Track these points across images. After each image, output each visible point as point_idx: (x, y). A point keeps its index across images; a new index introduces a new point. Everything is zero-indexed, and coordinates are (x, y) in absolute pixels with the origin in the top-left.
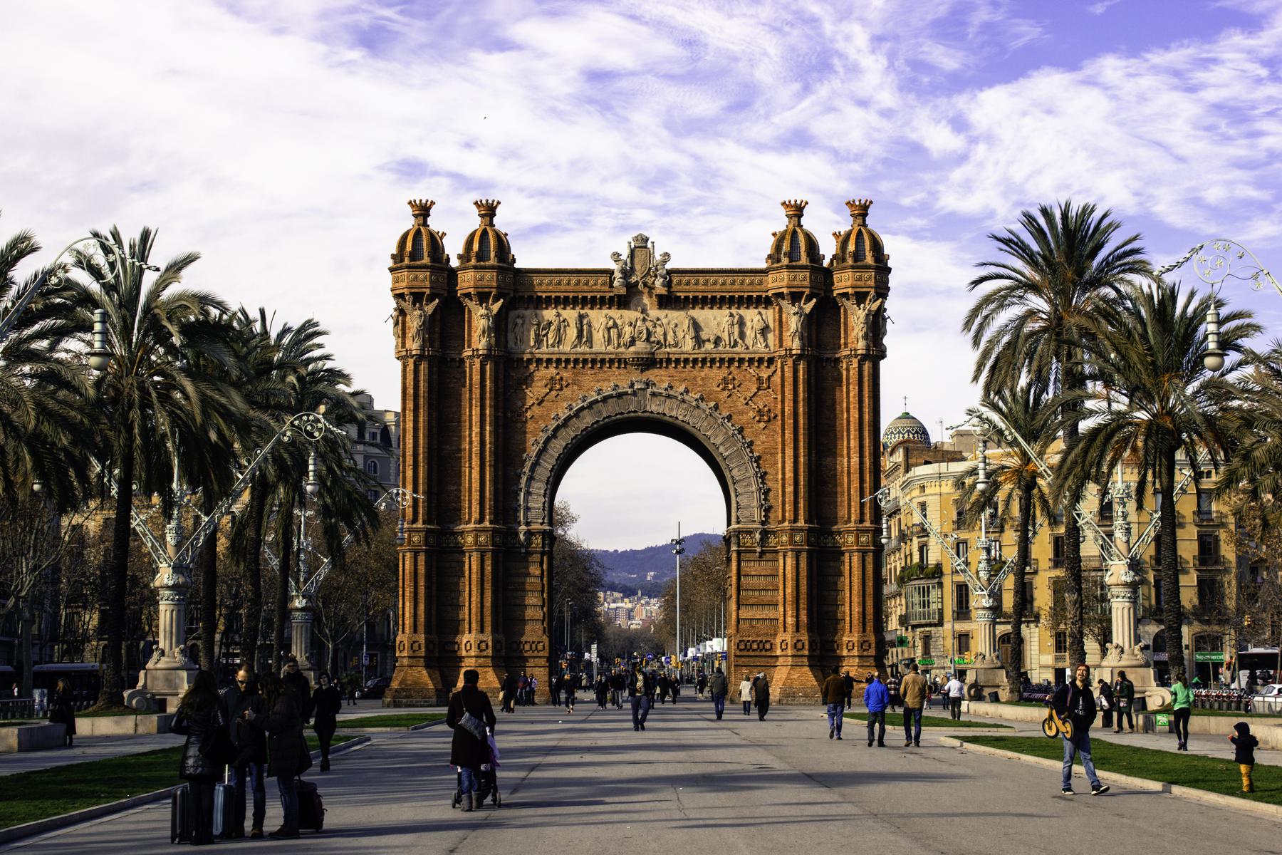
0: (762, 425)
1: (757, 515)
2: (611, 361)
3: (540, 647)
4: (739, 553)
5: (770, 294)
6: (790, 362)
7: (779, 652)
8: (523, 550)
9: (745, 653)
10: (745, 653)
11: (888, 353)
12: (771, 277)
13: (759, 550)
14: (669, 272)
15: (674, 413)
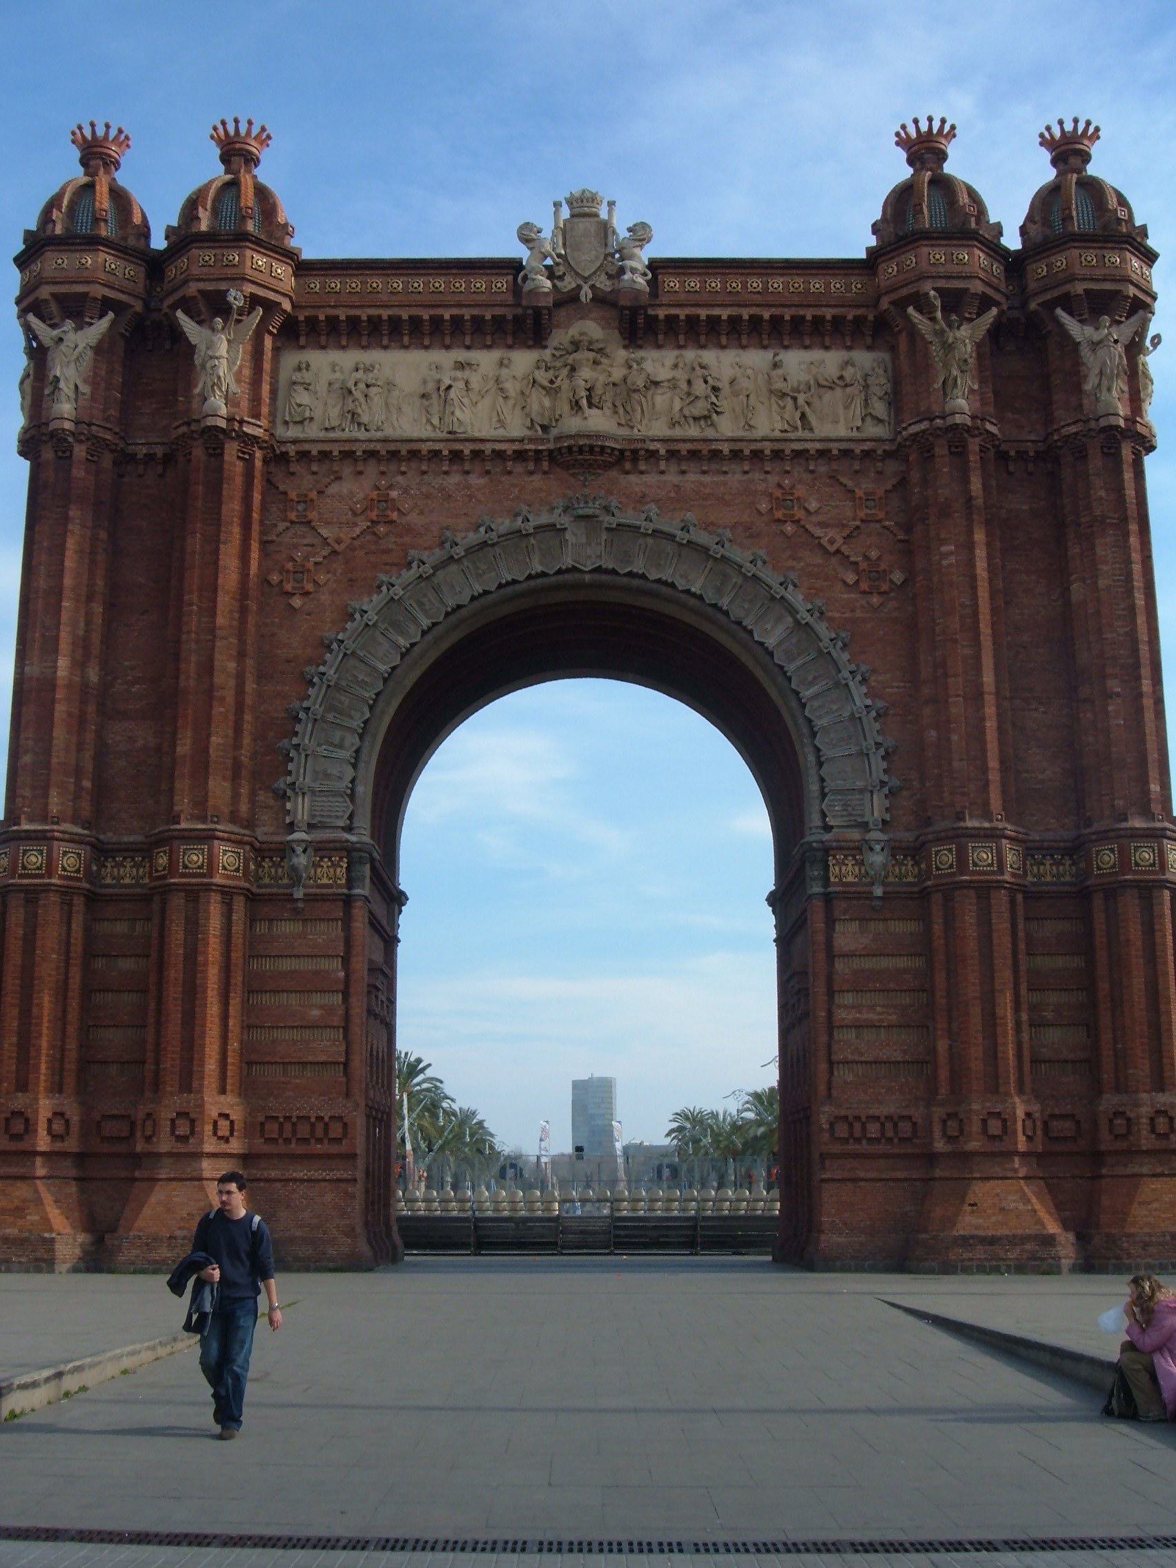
0: (875, 600)
1: (876, 807)
2: (520, 456)
3: (336, 1130)
4: (828, 899)
5: (885, 304)
6: (941, 450)
7: (940, 1145)
8: (299, 893)
9: (852, 1147)
10: (852, 1147)
11: (1160, 441)
12: (890, 270)
13: (878, 891)
14: (656, 266)
15: (666, 575)
